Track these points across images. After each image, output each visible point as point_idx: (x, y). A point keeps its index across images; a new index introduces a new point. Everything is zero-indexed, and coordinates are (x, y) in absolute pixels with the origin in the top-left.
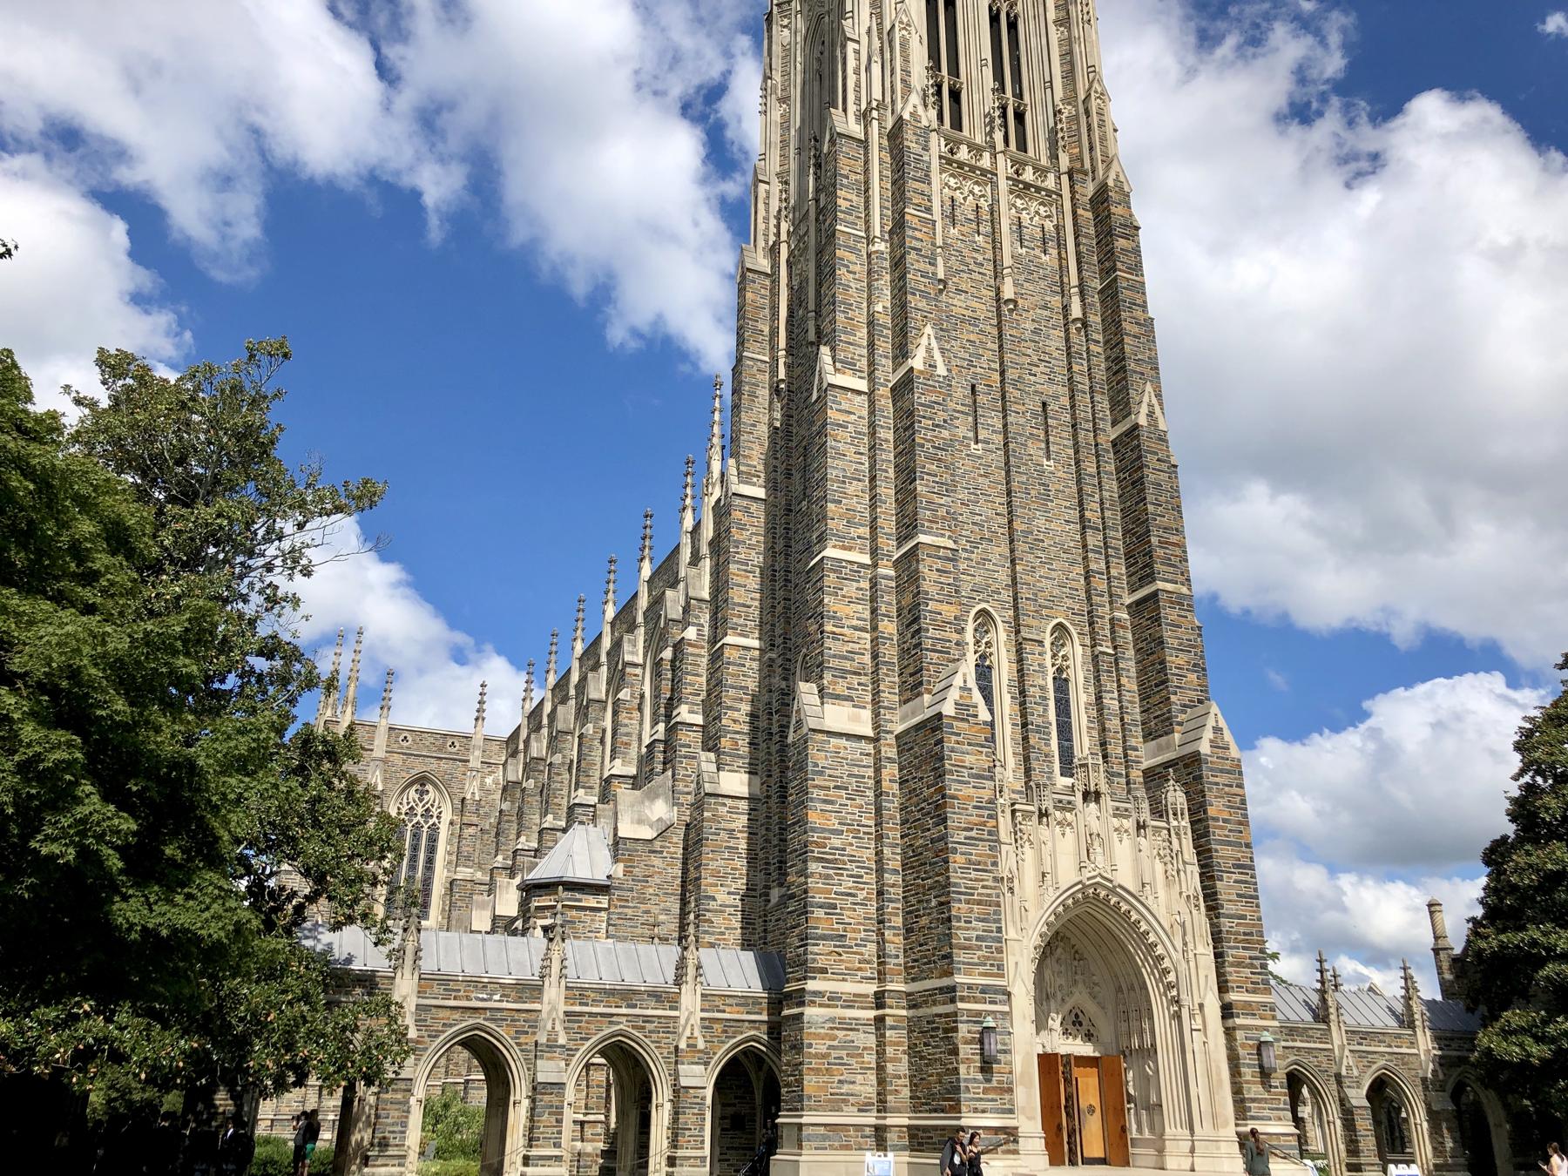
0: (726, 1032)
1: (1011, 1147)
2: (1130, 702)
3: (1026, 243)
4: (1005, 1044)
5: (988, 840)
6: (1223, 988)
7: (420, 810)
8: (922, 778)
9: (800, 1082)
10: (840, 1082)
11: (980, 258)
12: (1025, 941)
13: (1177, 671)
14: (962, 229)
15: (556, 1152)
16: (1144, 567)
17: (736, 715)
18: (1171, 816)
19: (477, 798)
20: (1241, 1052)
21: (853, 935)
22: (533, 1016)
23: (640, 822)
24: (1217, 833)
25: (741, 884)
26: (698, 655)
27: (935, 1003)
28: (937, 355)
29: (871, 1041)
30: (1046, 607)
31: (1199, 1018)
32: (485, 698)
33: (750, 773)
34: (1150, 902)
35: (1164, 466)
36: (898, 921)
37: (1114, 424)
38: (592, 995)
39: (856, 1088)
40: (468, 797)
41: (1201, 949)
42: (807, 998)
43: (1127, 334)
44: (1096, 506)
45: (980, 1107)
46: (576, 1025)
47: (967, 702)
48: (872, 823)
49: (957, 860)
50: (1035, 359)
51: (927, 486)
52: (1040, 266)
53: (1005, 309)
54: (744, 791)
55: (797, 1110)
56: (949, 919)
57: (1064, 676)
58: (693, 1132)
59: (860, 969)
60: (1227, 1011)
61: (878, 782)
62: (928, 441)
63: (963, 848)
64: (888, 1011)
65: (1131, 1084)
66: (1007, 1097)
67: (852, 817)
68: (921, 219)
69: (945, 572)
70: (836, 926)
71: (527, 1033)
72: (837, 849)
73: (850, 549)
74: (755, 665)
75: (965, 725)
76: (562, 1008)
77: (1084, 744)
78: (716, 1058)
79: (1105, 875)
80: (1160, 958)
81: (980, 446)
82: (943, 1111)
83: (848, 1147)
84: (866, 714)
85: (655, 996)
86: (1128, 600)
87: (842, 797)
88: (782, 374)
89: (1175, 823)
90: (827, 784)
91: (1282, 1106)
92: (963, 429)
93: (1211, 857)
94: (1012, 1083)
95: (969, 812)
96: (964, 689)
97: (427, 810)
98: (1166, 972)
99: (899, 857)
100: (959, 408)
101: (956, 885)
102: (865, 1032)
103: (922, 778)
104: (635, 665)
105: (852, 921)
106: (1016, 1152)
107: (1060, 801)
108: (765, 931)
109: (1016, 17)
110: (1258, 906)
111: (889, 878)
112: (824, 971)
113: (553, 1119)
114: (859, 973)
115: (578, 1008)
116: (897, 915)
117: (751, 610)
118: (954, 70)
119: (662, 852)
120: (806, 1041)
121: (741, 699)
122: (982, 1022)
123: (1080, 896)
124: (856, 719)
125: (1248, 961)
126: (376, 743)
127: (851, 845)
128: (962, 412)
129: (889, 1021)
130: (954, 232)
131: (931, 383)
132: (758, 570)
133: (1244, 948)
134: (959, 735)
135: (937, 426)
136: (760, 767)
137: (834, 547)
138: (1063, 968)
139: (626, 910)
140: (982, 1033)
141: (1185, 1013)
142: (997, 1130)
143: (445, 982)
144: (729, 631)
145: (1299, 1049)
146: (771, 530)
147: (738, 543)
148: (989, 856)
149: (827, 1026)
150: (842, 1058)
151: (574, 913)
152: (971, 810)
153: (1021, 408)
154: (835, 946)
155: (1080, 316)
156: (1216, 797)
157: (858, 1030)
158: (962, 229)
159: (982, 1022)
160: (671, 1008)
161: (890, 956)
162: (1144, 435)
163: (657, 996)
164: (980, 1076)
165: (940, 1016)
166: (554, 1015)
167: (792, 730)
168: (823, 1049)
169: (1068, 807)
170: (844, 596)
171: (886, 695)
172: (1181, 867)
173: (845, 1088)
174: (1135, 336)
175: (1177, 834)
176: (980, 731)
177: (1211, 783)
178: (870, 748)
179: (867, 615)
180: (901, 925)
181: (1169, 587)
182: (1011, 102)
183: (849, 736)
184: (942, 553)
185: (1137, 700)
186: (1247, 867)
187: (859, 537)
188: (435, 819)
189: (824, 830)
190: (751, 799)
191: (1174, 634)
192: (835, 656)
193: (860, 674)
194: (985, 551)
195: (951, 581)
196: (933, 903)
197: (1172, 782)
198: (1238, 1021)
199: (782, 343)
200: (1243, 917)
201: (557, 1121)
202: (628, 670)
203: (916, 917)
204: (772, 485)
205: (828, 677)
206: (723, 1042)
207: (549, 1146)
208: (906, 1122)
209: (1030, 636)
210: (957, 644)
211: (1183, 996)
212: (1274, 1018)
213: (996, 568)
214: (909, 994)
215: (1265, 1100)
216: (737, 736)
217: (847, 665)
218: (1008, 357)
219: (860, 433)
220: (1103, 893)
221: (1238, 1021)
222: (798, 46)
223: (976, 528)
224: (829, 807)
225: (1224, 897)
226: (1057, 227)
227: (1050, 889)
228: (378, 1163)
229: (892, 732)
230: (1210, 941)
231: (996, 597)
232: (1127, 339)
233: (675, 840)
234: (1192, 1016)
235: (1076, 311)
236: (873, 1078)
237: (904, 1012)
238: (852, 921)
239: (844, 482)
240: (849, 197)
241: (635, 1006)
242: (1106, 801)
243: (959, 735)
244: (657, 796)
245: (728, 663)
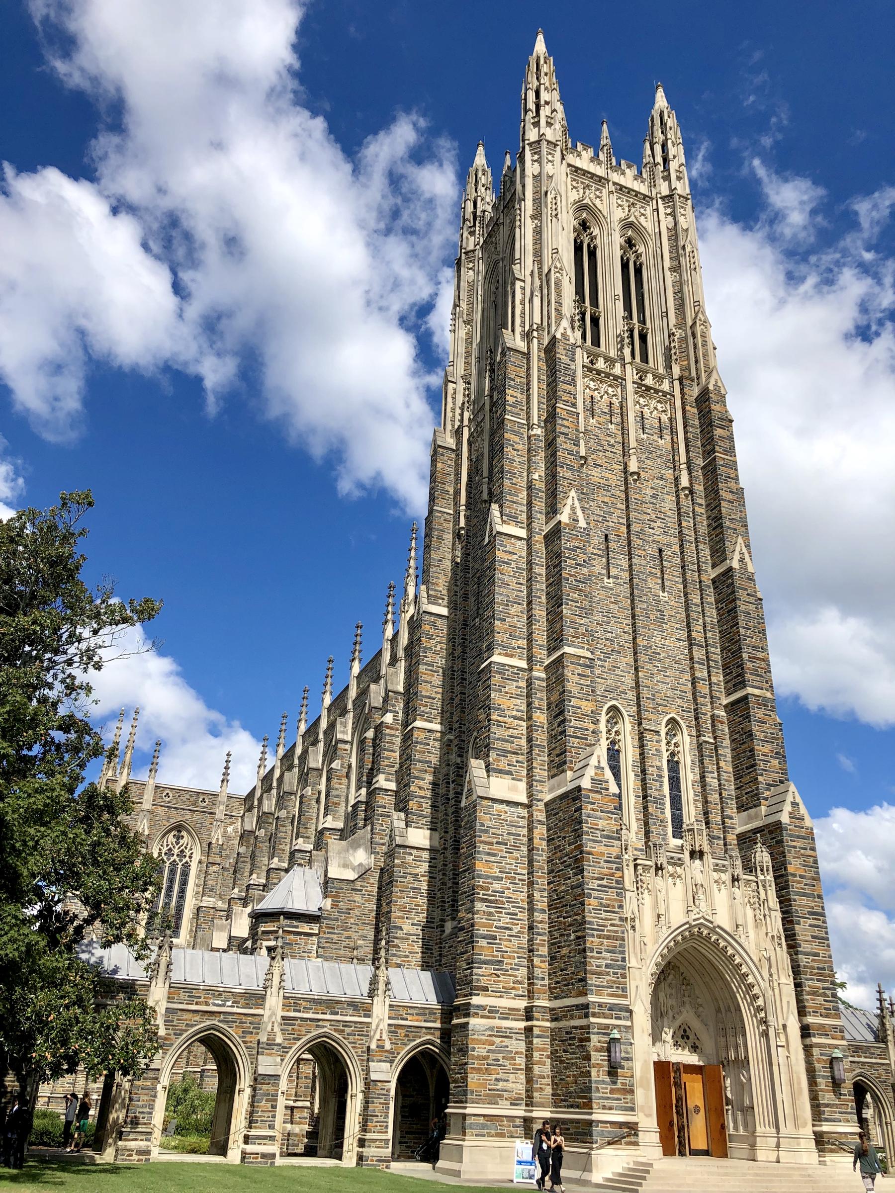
0: (407, 1036)
1: (633, 1139)
2: (727, 781)
3: (647, 431)
4: (627, 1053)
5: (616, 888)
6: (802, 1012)
7: (176, 851)
8: (565, 837)
9: (465, 1079)
10: (497, 1080)
11: (612, 441)
12: (644, 969)
13: (763, 758)
14: (599, 419)
15: (270, 1133)
16: (738, 676)
17: (421, 783)
18: (759, 872)
19: (220, 843)
20: (818, 1066)
21: (509, 961)
22: (256, 1019)
23: (345, 866)
24: (796, 886)
25: (422, 917)
26: (393, 736)
27: (572, 1018)
28: (579, 512)
29: (522, 1046)
31: (782, 1036)
32: (230, 765)
33: (431, 829)
34: (742, 940)
35: (752, 599)
36: (544, 951)
37: (714, 566)
38: (304, 1003)
39: (509, 1085)
40: (214, 842)
41: (783, 980)
42: (472, 1011)
43: (723, 500)
44: (701, 629)
45: (608, 1105)
46: (291, 1027)
48: (525, 872)
49: (591, 903)
50: (653, 516)
51: (570, 609)
52: (658, 448)
53: (630, 479)
54: (426, 843)
55: (462, 1102)
56: (584, 950)
57: (676, 759)
58: (379, 1119)
59: (513, 988)
60: (806, 1031)
61: (531, 840)
62: (572, 576)
63: (595, 894)
64: (535, 1023)
65: (729, 1089)
66: (629, 1097)
67: (510, 867)
69: (585, 676)
70: (496, 953)
71: (252, 1033)
72: (497, 892)
73: (511, 656)
74: (437, 744)
76: (280, 1013)
77: (691, 813)
78: (399, 1057)
79: (707, 917)
80: (751, 986)
81: (611, 580)
82: (578, 1107)
83: (501, 1135)
84: (522, 786)
85: (353, 1006)
86: (725, 701)
87: (502, 851)
88: (462, 523)
89: (762, 877)
90: (490, 840)
91: (849, 1110)
92: (598, 566)
93: (790, 905)
94: (633, 1085)
95: (601, 865)
96: (599, 767)
97: (182, 851)
98: (755, 997)
99: (545, 899)
100: (595, 551)
101: (590, 923)
102: (517, 1039)
103: (565, 837)
104: (345, 742)
105: (509, 950)
106: (636, 1144)
107: (672, 858)
108: (440, 955)
109: (641, 265)
110: (828, 946)
111: (538, 916)
112: (485, 989)
113: (269, 1105)
114: (513, 992)
115: (292, 1014)
116: (543, 945)
117: (435, 701)
118: (595, 302)
119: (361, 890)
120: (470, 1046)
121: (426, 771)
122: (609, 1034)
123: (687, 933)
124: (514, 789)
125: (821, 991)
126: (145, 797)
127: (509, 889)
128: (598, 555)
129: (536, 1031)
131: (574, 532)
132: (441, 670)
133: (818, 980)
134: (594, 804)
135: (579, 565)
136: (439, 825)
137: (500, 654)
138: (673, 991)
139: (332, 936)
140: (609, 1043)
141: (771, 1032)
142: (621, 1125)
143: (188, 990)
144: (418, 717)
145: (863, 1063)
146: (451, 639)
147: (426, 650)
148: (616, 900)
149: (487, 1033)
150: (498, 1060)
151: (292, 937)
152: (602, 861)
153: (643, 553)
154: (495, 969)
155: (688, 485)
156: (794, 857)
157: (511, 1037)
158: (599, 419)
159: (609, 1034)
160: (366, 1016)
161: (538, 979)
162: (737, 576)
163: (355, 1006)
164: (607, 1079)
165: (576, 1027)
166: (273, 1020)
167: (464, 796)
168: (484, 1053)
169: (679, 863)
170: (506, 693)
171: (538, 770)
172: (767, 912)
173: (500, 1086)
174: (729, 501)
175: (764, 886)
176: (611, 801)
177: (790, 846)
178: (524, 812)
179: (524, 707)
180: (546, 954)
181: (757, 692)
182: (636, 326)
183: (508, 803)
184: (582, 661)
185: (732, 779)
186: (819, 915)
187: (518, 647)
188: (187, 858)
189: (488, 877)
190: (432, 850)
191: (761, 729)
192: (498, 739)
193: (518, 754)
194: (615, 661)
195: (589, 683)
196: (572, 937)
197: (759, 845)
198: (815, 1040)
199: (463, 501)
200: (817, 955)
201: (272, 1107)
202: (340, 746)
203: (559, 947)
204: (453, 606)
205: (493, 755)
206: (405, 1044)
207: (265, 1128)
208: (548, 1115)
209: (649, 727)
210: (593, 732)
211: (770, 1018)
212: (843, 1038)
214: (552, 1010)
215: (836, 1106)
216: (422, 800)
217: (508, 746)
218: (633, 515)
219: (520, 569)
220: (705, 932)
221: (815, 1040)
222: (480, 283)
223: (609, 643)
224: (492, 859)
225: (801, 938)
226: (670, 419)
227: (664, 928)
228: (130, 1137)
229: (542, 800)
230: (791, 973)
232: (723, 504)
233: (372, 881)
234: (777, 1034)
235: (685, 482)
236: (522, 1077)
237: (548, 1024)
238: (509, 950)
239: (508, 605)
240: (515, 394)
241: (337, 1013)
242: (709, 859)
243: (594, 804)
244: (359, 846)
245: (417, 743)
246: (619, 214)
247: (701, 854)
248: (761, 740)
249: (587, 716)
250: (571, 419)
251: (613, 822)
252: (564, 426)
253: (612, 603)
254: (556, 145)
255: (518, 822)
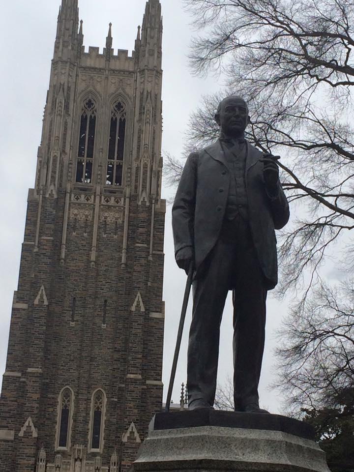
2: (119, 419)
3: (107, 232)
11: (84, 243)
28: (45, 298)
30: (94, 384)
47: (29, 431)
51: (33, 349)
68: (47, 240)
75: (27, 439)
81: (74, 323)
84: (12, 432)
96: (29, 426)
100: (67, 309)
107: (65, 462)
130: (74, 234)
131: (41, 309)
135: (42, 325)
153: (91, 306)
170: (9, 389)
174: (139, 272)
181: (132, 376)
182: (115, 163)
195: (38, 385)
213: (75, 371)
217: (8, 415)
223: (68, 356)
231: (73, 382)
239: (14, 346)
240: (30, 228)
242: (85, 462)
246: (112, 89)
247: (81, 460)
248: (130, 401)
249: (35, 400)
250: (48, 244)
251: (32, 450)
252: (44, 249)
253: (73, 335)
254: (67, 62)
255: (8, 448)
